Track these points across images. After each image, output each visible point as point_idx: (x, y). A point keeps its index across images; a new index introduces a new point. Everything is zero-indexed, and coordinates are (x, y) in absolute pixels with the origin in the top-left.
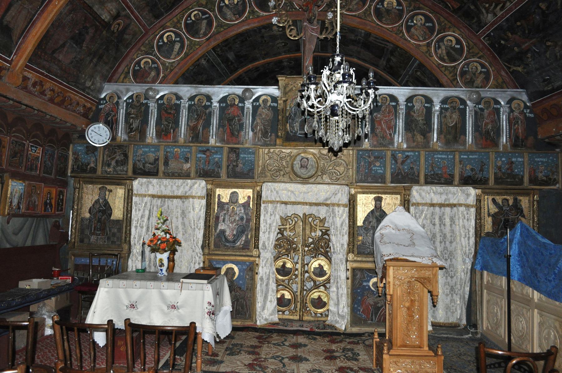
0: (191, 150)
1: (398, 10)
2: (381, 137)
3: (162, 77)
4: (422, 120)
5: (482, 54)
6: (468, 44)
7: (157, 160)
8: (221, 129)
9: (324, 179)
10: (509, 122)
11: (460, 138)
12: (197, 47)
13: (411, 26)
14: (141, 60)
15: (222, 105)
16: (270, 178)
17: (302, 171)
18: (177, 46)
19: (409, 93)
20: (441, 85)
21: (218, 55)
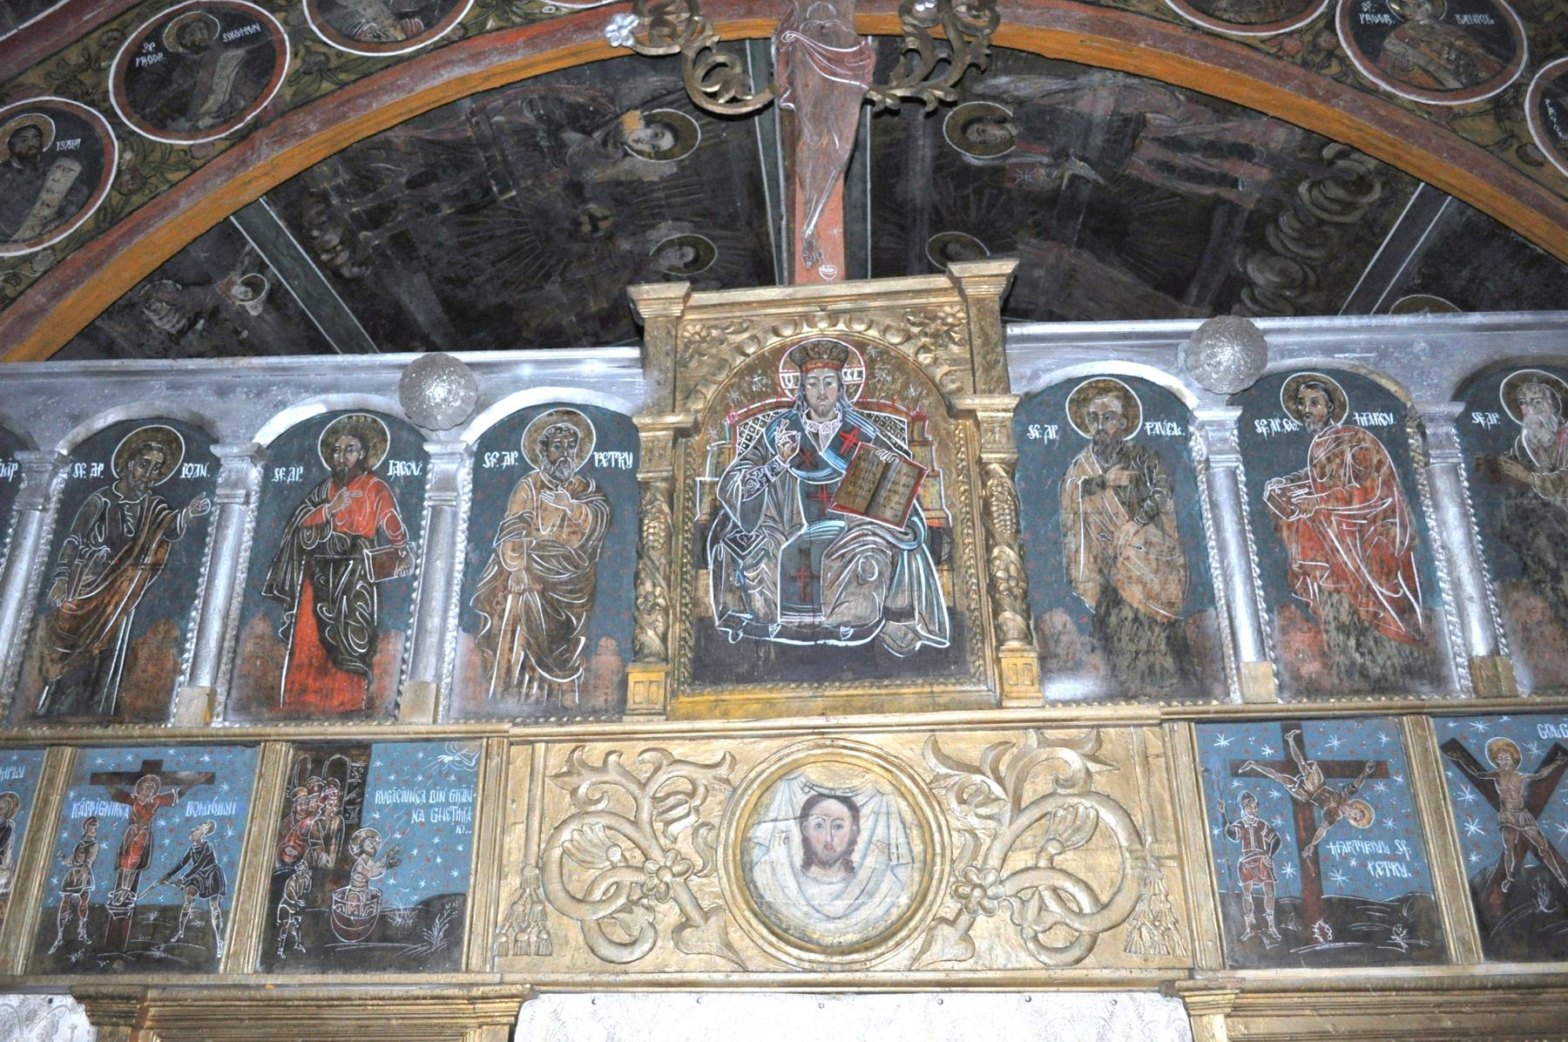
2: (1342, 628)
8: (260, 626)
9: (981, 945)
13: (1382, 30)
15: (279, 474)
16: (584, 956)
17: (813, 890)
18: (61, 179)
21: (335, 274)
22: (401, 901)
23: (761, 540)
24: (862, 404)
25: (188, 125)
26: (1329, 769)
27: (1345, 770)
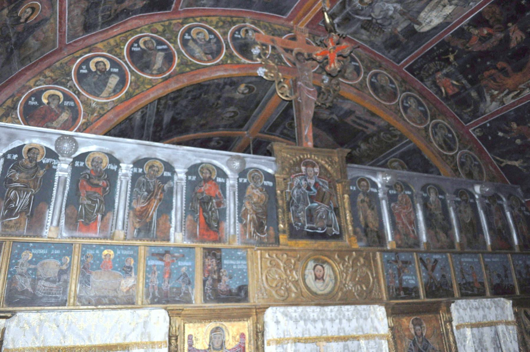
0: (137, 252)
2: (404, 235)
3: (83, 124)
4: (440, 214)
8: (190, 217)
12: (149, 87)
14: (41, 92)
17: (317, 284)
18: (114, 81)
22: (234, 286)
23: (301, 207)
24: (319, 177)
25: (150, 72)
27: (405, 263)
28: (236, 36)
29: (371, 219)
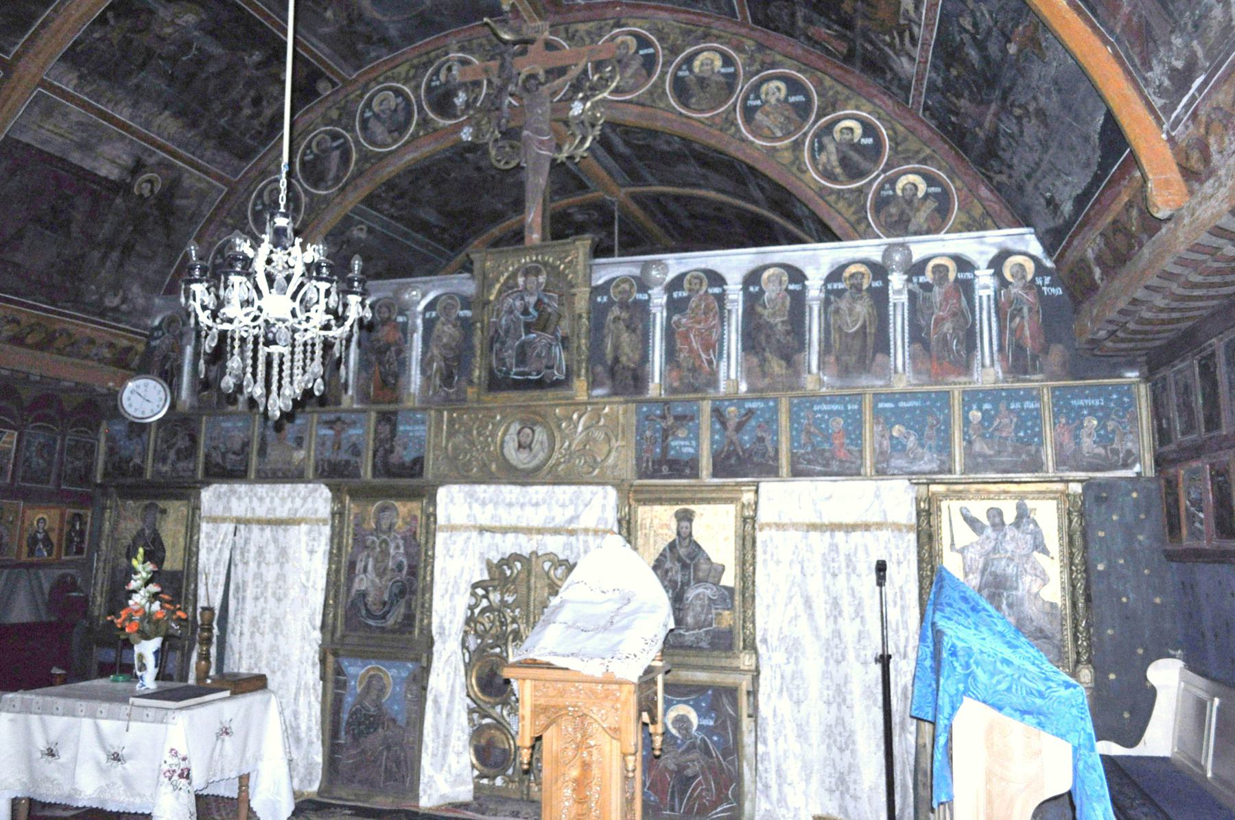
1: (726, 75)
2: (689, 370)
4: (783, 322)
5: (928, 151)
6: (895, 133)
7: (246, 444)
8: (364, 374)
10: (997, 313)
11: (873, 360)
13: (755, 108)
19: (752, 261)
20: (835, 238)
21: (392, 217)
22: (408, 457)
23: (509, 342)
24: (545, 290)
26: (677, 418)
27: (681, 419)
28: (433, 84)
29: (626, 349)
